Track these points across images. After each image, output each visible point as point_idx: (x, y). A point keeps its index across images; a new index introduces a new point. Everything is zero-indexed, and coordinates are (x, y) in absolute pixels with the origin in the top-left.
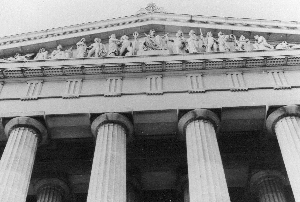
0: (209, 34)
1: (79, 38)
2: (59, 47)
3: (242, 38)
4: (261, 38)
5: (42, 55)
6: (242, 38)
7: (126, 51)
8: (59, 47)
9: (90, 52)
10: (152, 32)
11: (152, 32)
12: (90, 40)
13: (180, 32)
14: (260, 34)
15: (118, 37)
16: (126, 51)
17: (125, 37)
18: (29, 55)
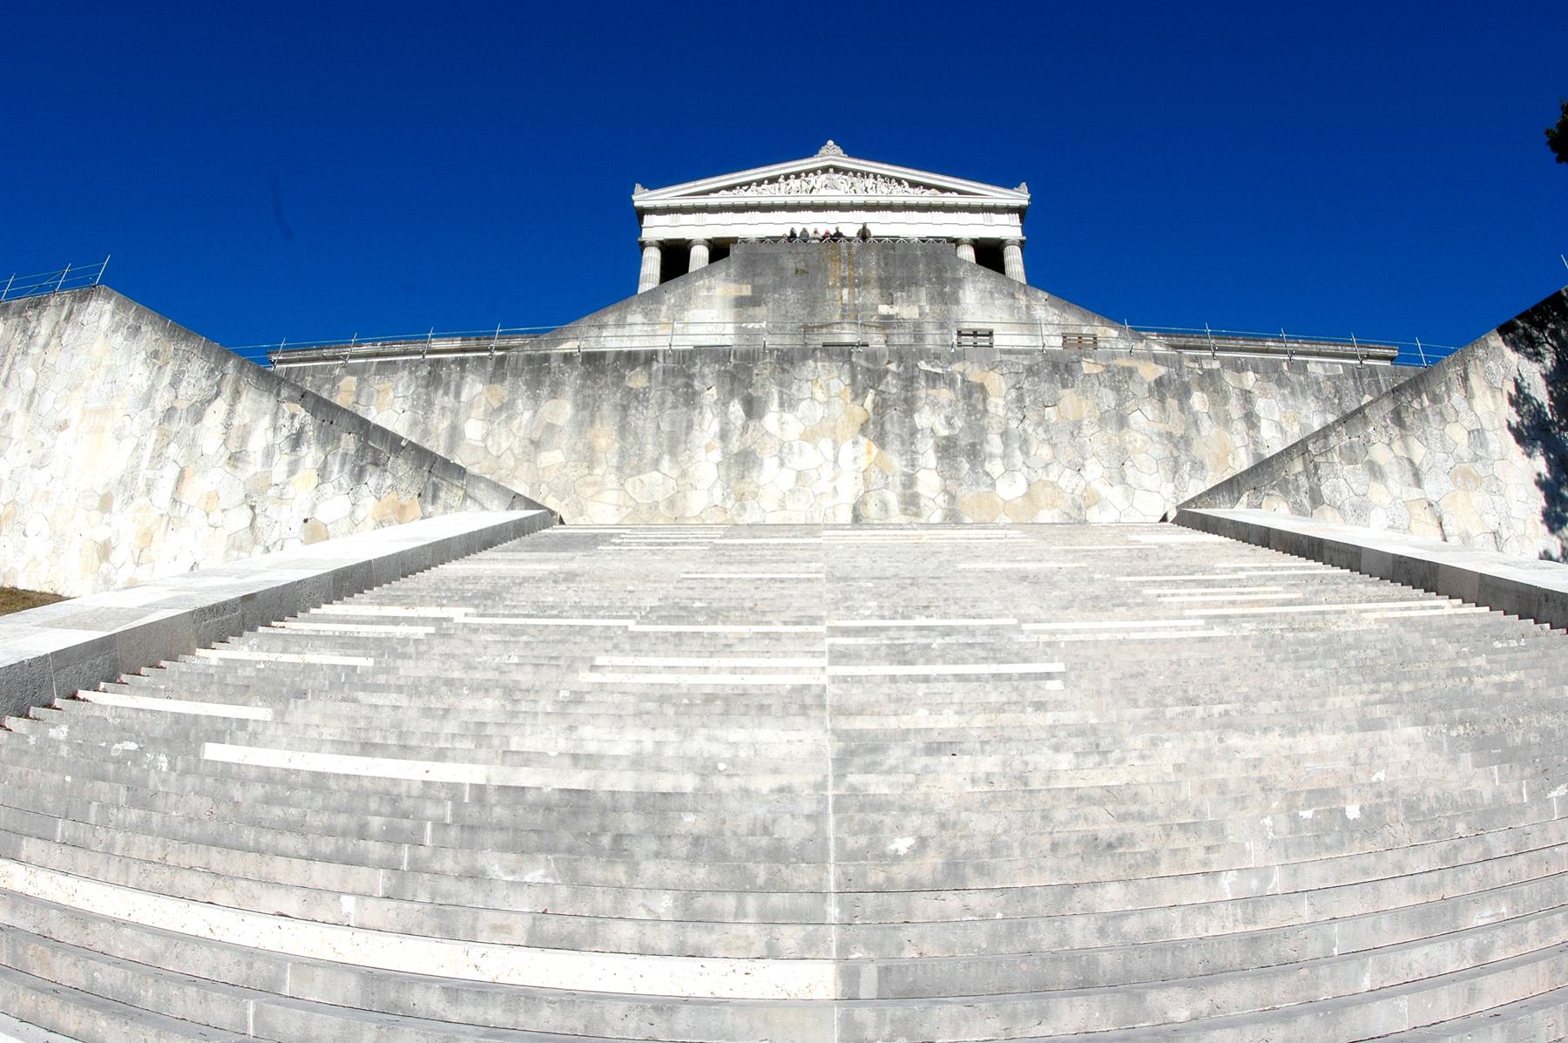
0: (871, 175)
1: (779, 177)
2: (766, 182)
3: (893, 180)
4: (906, 184)
5: (754, 187)
6: (893, 180)
7: (813, 188)
8: (766, 182)
9: (789, 187)
10: (831, 170)
11: (831, 170)
12: (787, 177)
13: (851, 173)
14: (906, 180)
15: (807, 176)
16: (813, 188)
17: (811, 174)
18: (746, 188)
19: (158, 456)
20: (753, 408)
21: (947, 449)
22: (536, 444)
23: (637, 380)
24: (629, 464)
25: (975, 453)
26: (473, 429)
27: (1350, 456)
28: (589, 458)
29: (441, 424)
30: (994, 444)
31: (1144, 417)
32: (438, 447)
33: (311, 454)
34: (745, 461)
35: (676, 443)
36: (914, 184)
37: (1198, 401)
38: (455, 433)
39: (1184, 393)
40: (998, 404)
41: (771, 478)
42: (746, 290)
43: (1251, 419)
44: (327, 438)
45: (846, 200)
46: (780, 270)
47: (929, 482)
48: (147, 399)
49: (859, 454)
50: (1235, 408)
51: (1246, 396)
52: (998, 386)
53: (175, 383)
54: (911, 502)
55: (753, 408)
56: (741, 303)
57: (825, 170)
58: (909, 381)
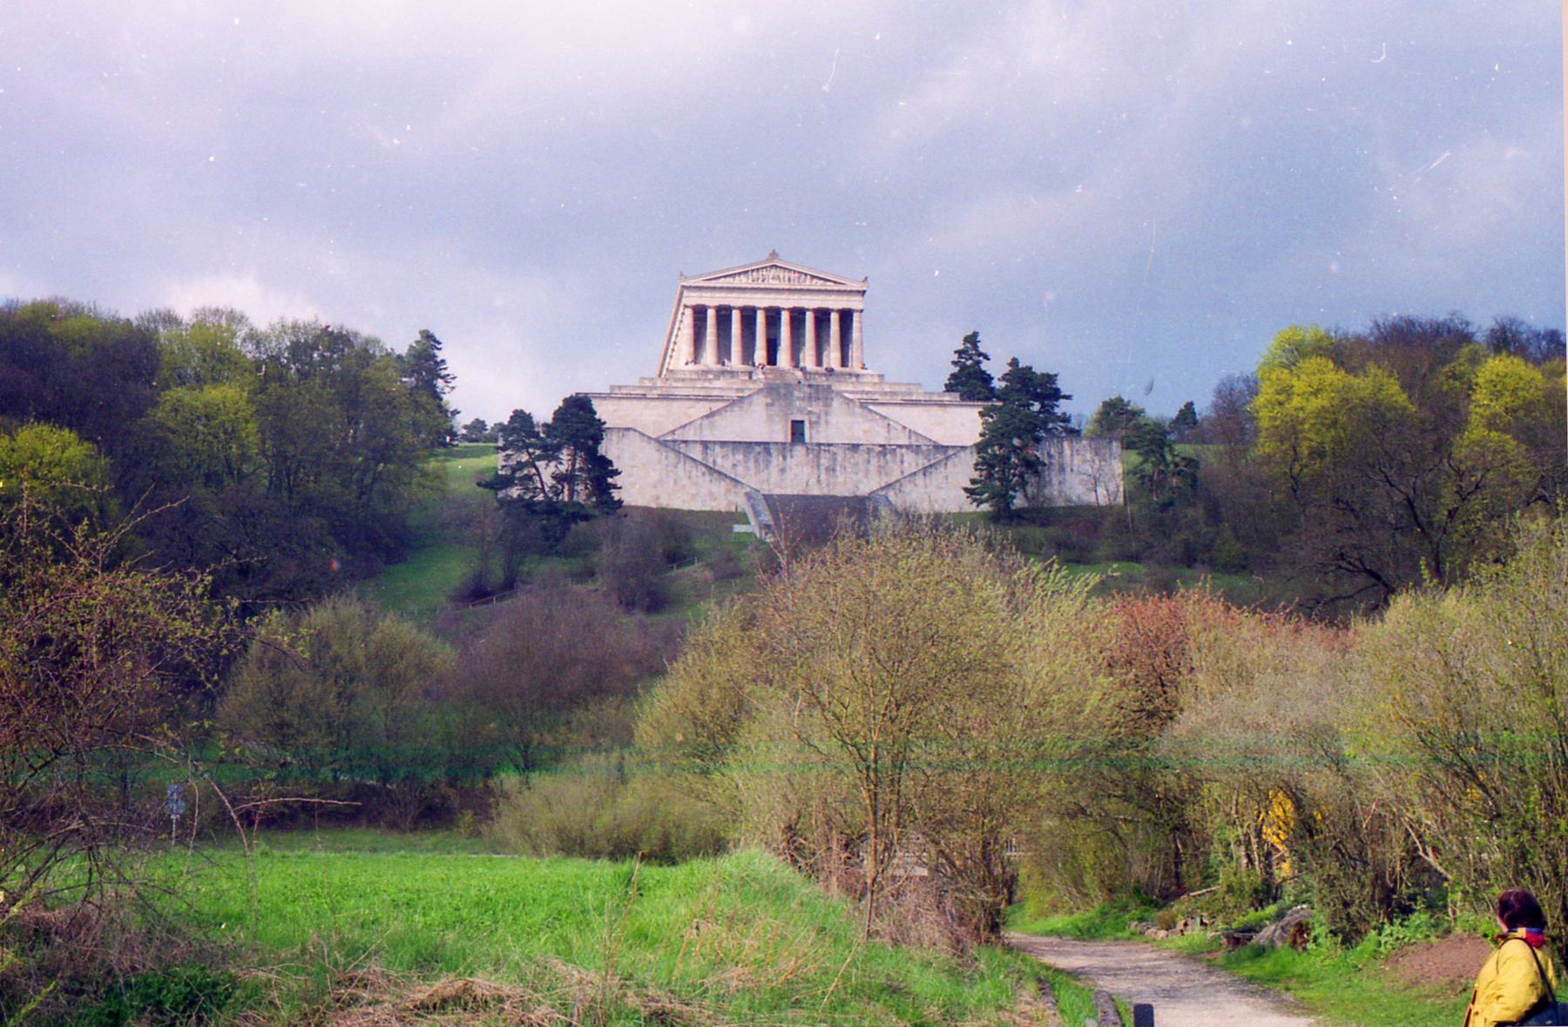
19: (667, 475)
20: (784, 458)
21: (827, 469)
22: (734, 465)
23: (758, 449)
24: (758, 471)
25: (834, 470)
26: (719, 461)
27: (910, 482)
28: (748, 469)
29: (711, 459)
30: (838, 468)
31: (874, 461)
32: (711, 465)
33: (707, 478)
34: (783, 471)
35: (767, 466)
36: (813, 277)
37: (889, 457)
38: (714, 462)
39: (885, 455)
40: (839, 458)
41: (789, 475)
42: (769, 400)
43: (902, 462)
44: (711, 475)
45: (780, 287)
46: (778, 393)
47: (823, 477)
48: (660, 462)
49: (807, 470)
50: (898, 459)
51: (902, 455)
52: (840, 454)
53: (666, 457)
54: (819, 481)
55: (784, 458)
56: (767, 405)
57: (771, 267)
58: (819, 452)
